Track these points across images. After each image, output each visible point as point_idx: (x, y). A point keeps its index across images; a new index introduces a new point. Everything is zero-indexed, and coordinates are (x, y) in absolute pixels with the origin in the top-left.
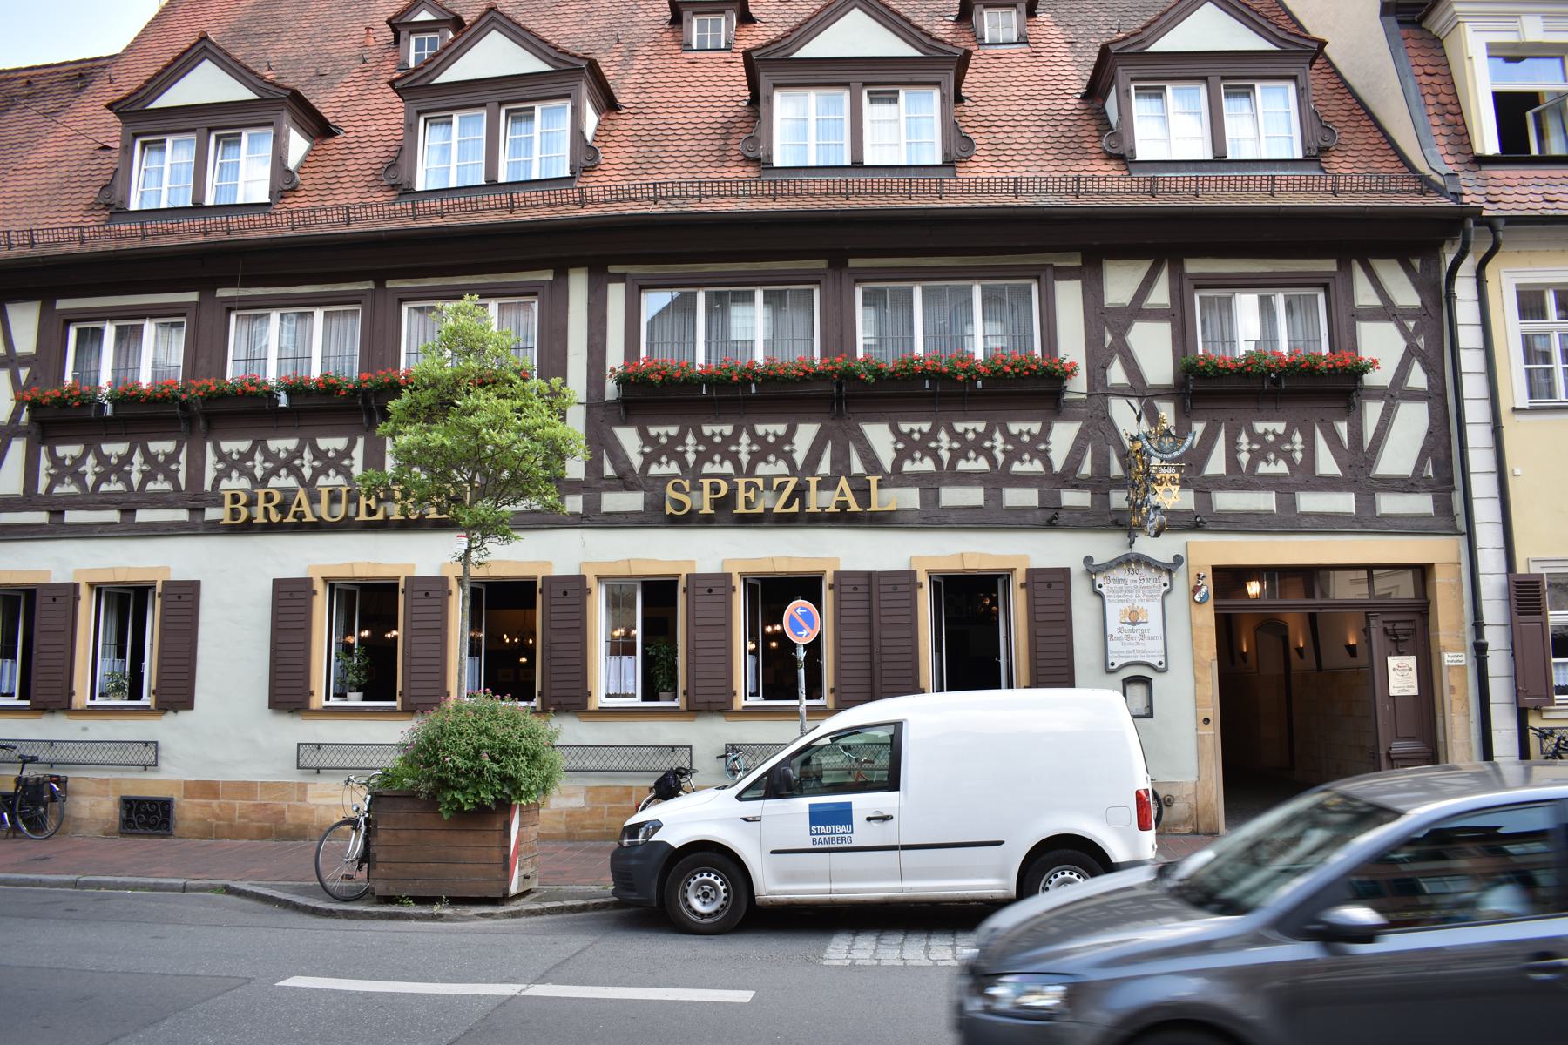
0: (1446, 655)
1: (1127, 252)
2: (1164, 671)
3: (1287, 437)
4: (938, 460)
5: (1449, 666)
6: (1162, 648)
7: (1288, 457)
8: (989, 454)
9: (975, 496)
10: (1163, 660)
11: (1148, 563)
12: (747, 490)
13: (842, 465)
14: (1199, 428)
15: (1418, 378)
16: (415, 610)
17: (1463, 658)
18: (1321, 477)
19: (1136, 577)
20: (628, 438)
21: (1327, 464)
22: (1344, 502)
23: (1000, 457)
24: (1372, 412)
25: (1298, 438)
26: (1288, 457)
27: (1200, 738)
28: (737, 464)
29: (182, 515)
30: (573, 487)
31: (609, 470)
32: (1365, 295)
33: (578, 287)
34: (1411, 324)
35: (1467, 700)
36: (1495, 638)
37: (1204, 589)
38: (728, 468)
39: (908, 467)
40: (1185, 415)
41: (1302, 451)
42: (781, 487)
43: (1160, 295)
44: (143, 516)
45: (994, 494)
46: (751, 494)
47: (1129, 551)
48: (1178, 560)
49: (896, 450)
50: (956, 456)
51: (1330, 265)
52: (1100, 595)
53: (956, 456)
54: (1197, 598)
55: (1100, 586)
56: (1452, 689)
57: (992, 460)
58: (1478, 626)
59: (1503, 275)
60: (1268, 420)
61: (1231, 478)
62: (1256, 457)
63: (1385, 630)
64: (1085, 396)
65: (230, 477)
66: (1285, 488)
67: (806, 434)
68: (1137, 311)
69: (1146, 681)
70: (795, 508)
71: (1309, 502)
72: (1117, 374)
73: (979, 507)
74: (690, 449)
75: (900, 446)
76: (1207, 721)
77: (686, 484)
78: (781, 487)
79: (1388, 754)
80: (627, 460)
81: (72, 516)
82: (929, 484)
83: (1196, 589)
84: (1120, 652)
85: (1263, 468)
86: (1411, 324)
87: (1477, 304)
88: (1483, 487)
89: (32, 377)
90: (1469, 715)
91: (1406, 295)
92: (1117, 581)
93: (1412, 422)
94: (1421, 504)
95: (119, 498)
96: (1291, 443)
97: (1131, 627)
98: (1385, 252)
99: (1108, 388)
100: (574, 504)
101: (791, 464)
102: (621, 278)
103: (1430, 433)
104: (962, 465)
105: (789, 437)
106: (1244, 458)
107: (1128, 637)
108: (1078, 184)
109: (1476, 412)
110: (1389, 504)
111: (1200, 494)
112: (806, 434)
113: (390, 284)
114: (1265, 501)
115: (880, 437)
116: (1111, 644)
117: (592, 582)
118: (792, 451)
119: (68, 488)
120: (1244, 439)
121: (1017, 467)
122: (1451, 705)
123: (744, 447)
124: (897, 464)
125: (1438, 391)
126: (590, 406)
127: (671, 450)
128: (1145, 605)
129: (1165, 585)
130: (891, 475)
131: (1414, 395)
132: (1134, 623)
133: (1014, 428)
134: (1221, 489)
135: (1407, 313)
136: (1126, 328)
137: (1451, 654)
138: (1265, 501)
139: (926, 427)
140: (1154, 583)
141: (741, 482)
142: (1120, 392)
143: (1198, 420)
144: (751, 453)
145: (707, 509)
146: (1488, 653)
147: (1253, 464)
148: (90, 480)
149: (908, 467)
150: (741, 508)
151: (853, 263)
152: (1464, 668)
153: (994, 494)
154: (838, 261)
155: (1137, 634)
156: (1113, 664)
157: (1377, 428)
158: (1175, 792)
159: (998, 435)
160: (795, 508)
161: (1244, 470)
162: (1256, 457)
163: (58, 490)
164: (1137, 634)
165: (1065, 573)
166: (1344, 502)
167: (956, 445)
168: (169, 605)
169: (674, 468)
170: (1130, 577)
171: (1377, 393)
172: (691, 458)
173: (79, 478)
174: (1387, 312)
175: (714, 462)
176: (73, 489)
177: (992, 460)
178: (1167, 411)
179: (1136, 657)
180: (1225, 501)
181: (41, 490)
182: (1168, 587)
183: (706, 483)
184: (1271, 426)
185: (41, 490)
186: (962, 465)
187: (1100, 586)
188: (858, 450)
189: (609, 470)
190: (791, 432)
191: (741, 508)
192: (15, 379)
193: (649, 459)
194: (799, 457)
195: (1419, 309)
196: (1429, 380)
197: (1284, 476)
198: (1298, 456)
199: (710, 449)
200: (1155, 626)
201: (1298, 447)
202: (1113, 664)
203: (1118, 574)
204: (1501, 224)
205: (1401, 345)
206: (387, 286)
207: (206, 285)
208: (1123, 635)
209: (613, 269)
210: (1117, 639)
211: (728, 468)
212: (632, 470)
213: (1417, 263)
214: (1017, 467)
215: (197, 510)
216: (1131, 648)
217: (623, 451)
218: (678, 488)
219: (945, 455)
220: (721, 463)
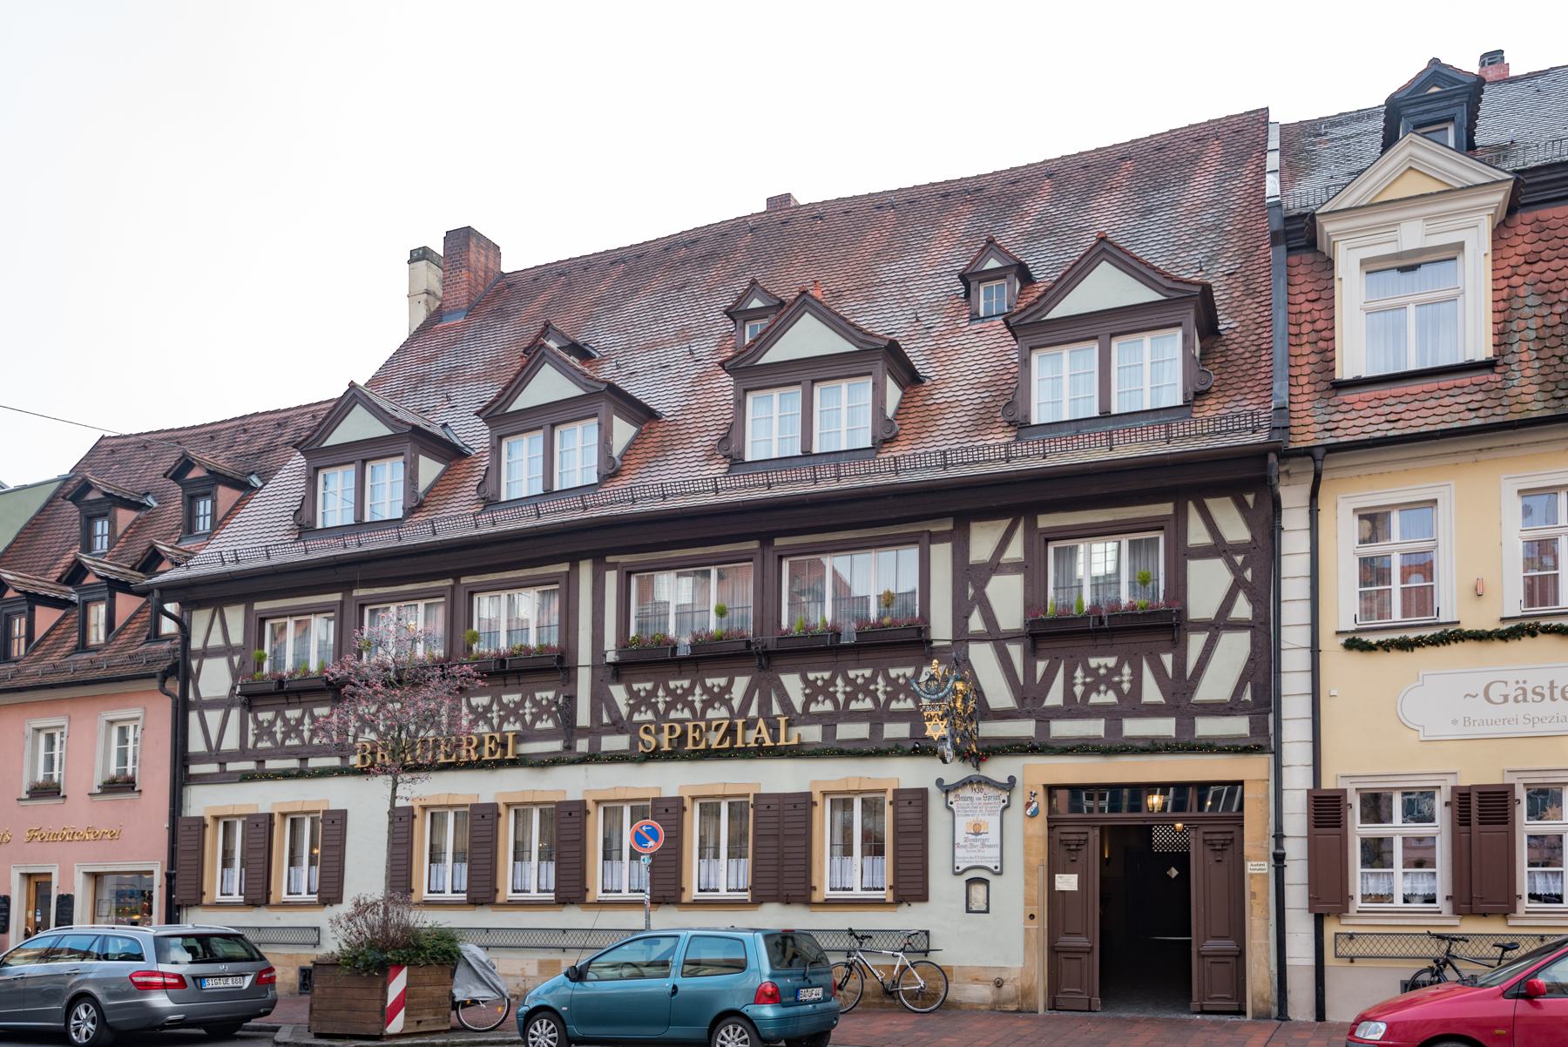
0: (1249, 864)
1: (988, 514)
2: (1000, 874)
3: (1117, 670)
4: (836, 702)
5: (1252, 875)
6: (957, 850)
7: (1117, 688)
8: (873, 695)
9: (861, 730)
10: (998, 865)
11: (988, 782)
12: (694, 731)
13: (765, 707)
14: (1041, 666)
15: (1243, 609)
17: (1266, 867)
18: (1146, 705)
19: (980, 795)
20: (619, 693)
21: (1152, 692)
22: (1165, 727)
23: (882, 697)
24: (1196, 642)
25: (1126, 670)
26: (1117, 688)
27: (1027, 931)
28: (693, 710)
29: (335, 762)
30: (584, 732)
31: (606, 720)
32: (1197, 534)
33: (586, 571)
34: (1239, 559)
35: (1267, 905)
37: (1034, 805)
38: (687, 714)
39: (813, 708)
40: (1031, 654)
41: (1131, 682)
42: (718, 728)
43: (1015, 551)
44: (313, 763)
45: (876, 729)
46: (697, 735)
47: (977, 773)
48: (1012, 780)
49: (806, 695)
50: (850, 697)
51: (1166, 509)
53: (850, 697)
54: (1029, 813)
55: (951, 803)
56: (1253, 895)
57: (876, 700)
58: (1279, 837)
59: (1341, 502)
60: (1102, 655)
61: (1067, 708)
62: (1090, 689)
63: (1204, 841)
64: (948, 643)
65: (364, 732)
66: (1113, 715)
67: (741, 684)
68: (995, 566)
69: (985, 882)
70: (726, 745)
71: (1134, 728)
72: (976, 623)
73: (865, 739)
74: (660, 700)
75: (807, 691)
76: (1032, 916)
77: (652, 728)
78: (718, 728)
80: (618, 711)
81: (231, 767)
82: (828, 722)
83: (1028, 805)
84: (964, 858)
85: (1095, 699)
86: (1239, 559)
87: (1308, 533)
88: (1295, 708)
89: (242, 662)
90: (1268, 919)
91: (1235, 529)
92: (965, 799)
93: (1234, 650)
94: (1238, 726)
95: (298, 750)
96: (1121, 675)
97: (974, 837)
98: (1218, 490)
100: (582, 746)
101: (731, 709)
102: (613, 566)
103: (1251, 659)
104: (854, 706)
105: (728, 689)
106: (1079, 690)
107: (972, 846)
108: (945, 458)
109: (1294, 635)
110: (1206, 727)
111: (1040, 724)
112: (741, 684)
113: (464, 580)
115: (793, 684)
116: (959, 852)
117: (591, 806)
118: (731, 699)
119: (265, 744)
120: (1079, 673)
121: (894, 705)
123: (698, 697)
124: (806, 706)
125: (1262, 620)
126: (594, 667)
127: (645, 702)
128: (986, 818)
129: (1004, 801)
130: (801, 715)
131: (1238, 626)
132: (977, 834)
133: (893, 673)
134: (1058, 717)
135: (1238, 548)
137: (1254, 863)
138: (1094, 728)
139: (827, 675)
140: (996, 798)
141: (690, 725)
142: (979, 638)
143: (1042, 659)
144: (703, 701)
145: (666, 747)
146: (1286, 863)
147: (1086, 695)
148: (279, 737)
149: (813, 708)
150: (690, 746)
151: (779, 542)
152: (1267, 875)
153: (876, 729)
154: (766, 539)
155: (979, 843)
156: (958, 868)
158: (1004, 977)
159: (880, 680)
161: (1079, 700)
162: (1090, 689)
163: (260, 745)
164: (979, 843)
165: (923, 794)
166: (1165, 727)
167: (848, 689)
168: (326, 828)
169: (649, 716)
170: (975, 795)
171: (1201, 626)
172: (661, 707)
173: (272, 735)
174: (1219, 548)
175: (677, 710)
176: (268, 744)
177: (876, 700)
178: (1016, 652)
180: (1061, 729)
181: (250, 746)
183: (666, 726)
184: (1102, 661)
185: (250, 746)
186: (854, 706)
187: (951, 803)
188: (778, 696)
189: (606, 720)
190: (731, 683)
191: (690, 746)
192: (231, 663)
193: (634, 709)
194: (736, 704)
195: (1250, 543)
196: (1254, 610)
197: (1114, 705)
198: (1126, 687)
199: (677, 699)
200: (993, 836)
201: (1126, 678)
202: (958, 868)
203: (967, 792)
204: (1319, 453)
205: (1227, 578)
206: (462, 582)
207: (346, 587)
209: (610, 559)
211: (687, 714)
212: (621, 718)
213: (1250, 498)
214: (894, 705)
215: (344, 758)
216: (973, 855)
217: (616, 704)
218: (647, 731)
219: (841, 697)
220: (682, 710)
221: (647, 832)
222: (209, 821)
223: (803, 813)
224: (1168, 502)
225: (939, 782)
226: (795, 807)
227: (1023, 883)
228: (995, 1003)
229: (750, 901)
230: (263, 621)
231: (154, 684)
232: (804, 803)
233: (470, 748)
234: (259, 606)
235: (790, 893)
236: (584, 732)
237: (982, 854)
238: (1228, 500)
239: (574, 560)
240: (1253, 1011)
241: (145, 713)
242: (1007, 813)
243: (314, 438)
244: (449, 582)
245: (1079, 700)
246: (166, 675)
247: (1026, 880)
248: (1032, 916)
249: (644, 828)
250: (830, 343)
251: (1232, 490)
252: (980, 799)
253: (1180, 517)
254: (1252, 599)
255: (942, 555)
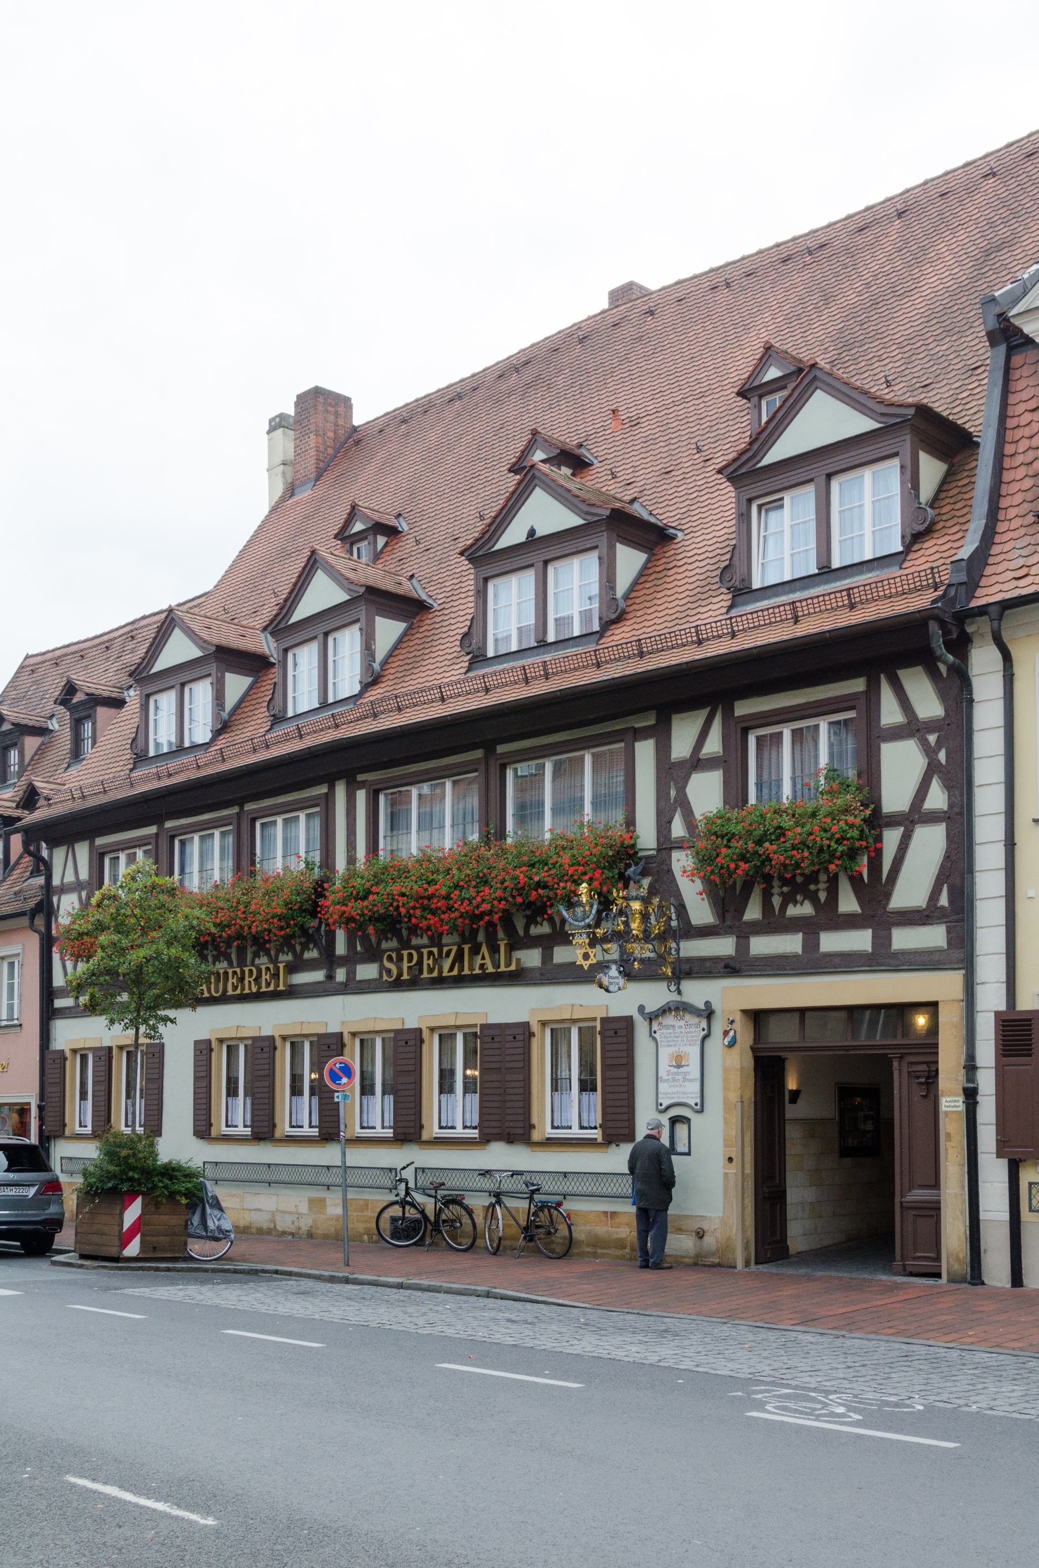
1: (687, 705)
5: (946, 1112)
7: (813, 898)
10: (698, 1101)
16: (257, 1062)
19: (682, 1023)
24: (891, 838)
27: (726, 1175)
32: (890, 713)
34: (932, 738)
36: (987, 1082)
37: (732, 1033)
43: (713, 745)
47: (678, 998)
51: (857, 685)
52: (655, 1039)
56: (948, 1136)
68: (696, 763)
69: (687, 1120)
70: (455, 972)
71: (831, 942)
77: (394, 955)
79: (901, 1203)
85: (792, 911)
86: (932, 738)
92: (667, 1027)
97: (675, 1070)
99: (672, 842)
102: (362, 785)
103: (947, 857)
107: (674, 1080)
110: (904, 939)
114: (791, 944)
116: (661, 1085)
122: (947, 1153)
130: (523, 938)
131: (933, 818)
132: (679, 1066)
135: (931, 726)
136: (686, 779)
137: (949, 1099)
140: (695, 1026)
146: (979, 1098)
151: (501, 749)
155: (680, 1077)
157: (895, 858)
160: (455, 972)
164: (680, 1077)
179: (678, 1098)
182: (705, 1032)
191: (425, 975)
195: (944, 719)
200: (693, 1069)
202: (661, 1105)
203: (669, 1020)
206: (246, 809)
207: (158, 819)
208: (670, 1077)
209: (360, 778)
210: (667, 1081)
216: (675, 1090)
218: (390, 958)
221: (341, 1068)
222: (68, 1054)
223: (625, 1039)
224: (860, 676)
225: (641, 1009)
226: (329, 1047)
227: (722, 1121)
228: (698, 1256)
229: (600, 1140)
230: (102, 856)
231: (25, 921)
232: (522, 1033)
233: (251, 979)
234: (100, 841)
235: (512, 1131)
236: (344, 961)
237: (682, 1089)
238: (920, 669)
239: (331, 781)
240: (948, 1273)
241: (23, 949)
242: (708, 1043)
243: (144, 664)
244: (235, 810)
245: (777, 910)
246: (34, 913)
247: (725, 1119)
248: (730, 1160)
249: (337, 1065)
250: (563, 518)
251: (926, 659)
252: (681, 1027)
253: (872, 696)
254: (948, 786)
255: (645, 751)
